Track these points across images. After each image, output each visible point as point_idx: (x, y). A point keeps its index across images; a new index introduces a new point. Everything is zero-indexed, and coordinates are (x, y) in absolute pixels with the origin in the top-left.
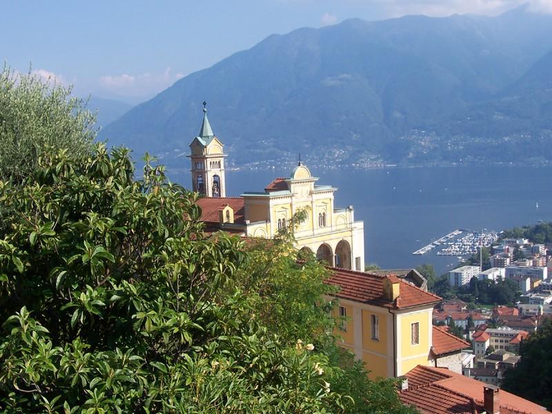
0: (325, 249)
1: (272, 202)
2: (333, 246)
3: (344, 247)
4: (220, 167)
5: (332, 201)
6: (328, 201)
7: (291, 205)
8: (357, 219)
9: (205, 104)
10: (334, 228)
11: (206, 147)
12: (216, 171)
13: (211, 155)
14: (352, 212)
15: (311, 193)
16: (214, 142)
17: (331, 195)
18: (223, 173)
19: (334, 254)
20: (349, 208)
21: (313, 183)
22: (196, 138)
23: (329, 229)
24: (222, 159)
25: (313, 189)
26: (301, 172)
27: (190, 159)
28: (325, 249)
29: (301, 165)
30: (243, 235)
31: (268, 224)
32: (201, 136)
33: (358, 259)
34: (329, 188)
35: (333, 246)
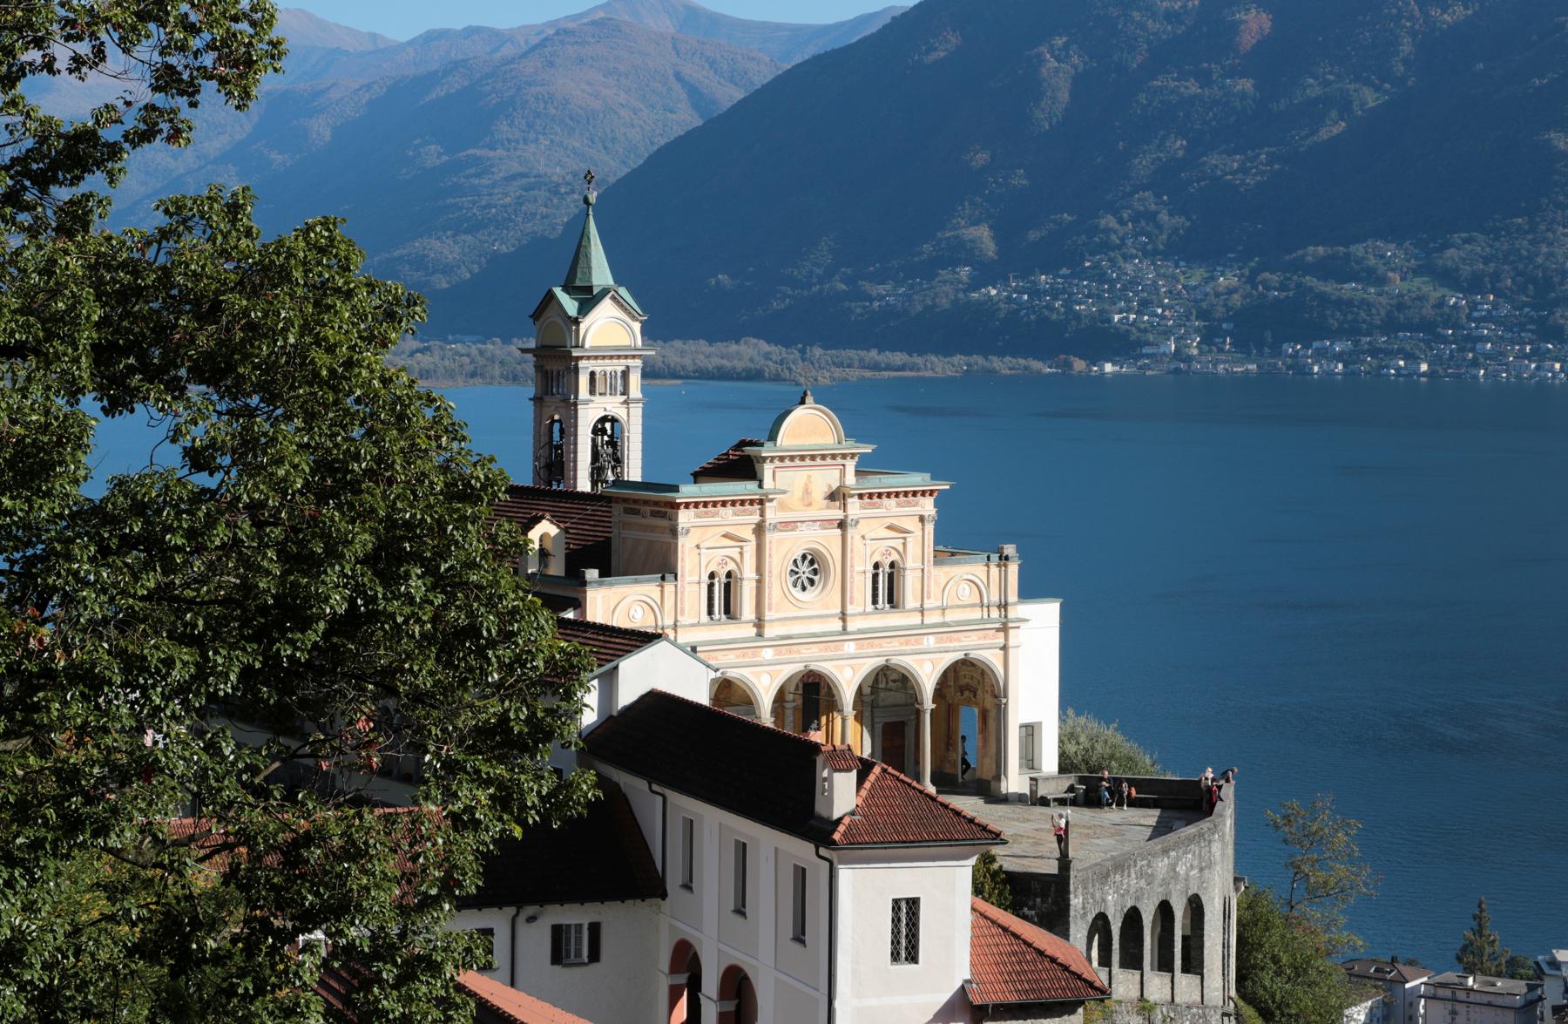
1: (685, 518)
2: (927, 676)
3: (971, 687)
4: (625, 392)
5: (930, 527)
6: (912, 524)
7: (759, 530)
8: (1029, 592)
10: (932, 618)
11: (576, 322)
12: (611, 405)
13: (593, 349)
14: (1013, 569)
15: (837, 496)
16: (606, 309)
17: (928, 506)
18: (637, 411)
19: (929, 704)
20: (1000, 551)
21: (851, 465)
22: (550, 296)
23: (915, 619)
24: (638, 362)
25: (851, 479)
26: (808, 425)
29: (809, 399)
30: (570, 615)
31: (669, 588)
32: (569, 288)
33: (1030, 732)
34: (918, 480)
35: (927, 676)
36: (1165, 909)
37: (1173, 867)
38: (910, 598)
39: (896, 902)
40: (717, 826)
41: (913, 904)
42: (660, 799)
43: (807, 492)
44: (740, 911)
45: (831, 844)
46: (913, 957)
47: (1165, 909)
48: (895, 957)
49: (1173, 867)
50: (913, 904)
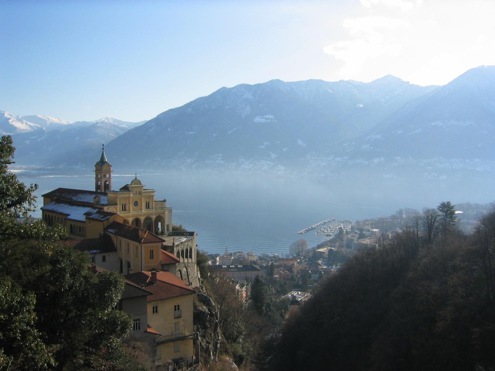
0: (148, 219)
9: (103, 145)
28: (148, 219)
35: (154, 217)
36: (187, 250)
37: (188, 244)
38: (151, 207)
39: (150, 251)
40: (124, 241)
41: (153, 251)
42: (116, 237)
43: (136, 192)
44: (128, 253)
45: (141, 243)
46: (153, 258)
47: (187, 250)
48: (150, 259)
49: (188, 244)
50: (153, 251)
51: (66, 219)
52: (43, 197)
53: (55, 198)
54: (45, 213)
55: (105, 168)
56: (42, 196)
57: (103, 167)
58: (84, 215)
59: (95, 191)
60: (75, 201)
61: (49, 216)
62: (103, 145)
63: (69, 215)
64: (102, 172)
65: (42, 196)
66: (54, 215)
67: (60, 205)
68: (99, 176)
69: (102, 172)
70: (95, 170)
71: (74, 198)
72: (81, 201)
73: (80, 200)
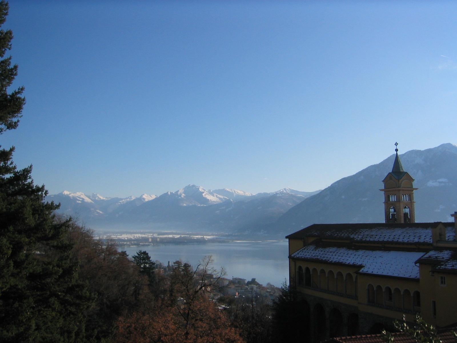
9: (396, 144)
27: (383, 192)
51: (357, 273)
52: (288, 240)
53: (311, 240)
54: (299, 264)
55: (404, 182)
56: (287, 237)
57: (401, 180)
58: (416, 263)
59: (385, 223)
60: (361, 241)
61: (307, 269)
62: (396, 144)
63: (361, 266)
64: (399, 190)
65: (287, 237)
66: (319, 268)
67: (327, 249)
68: (393, 199)
69: (399, 190)
70: (383, 188)
71: (357, 237)
72: (376, 240)
73: (371, 239)
